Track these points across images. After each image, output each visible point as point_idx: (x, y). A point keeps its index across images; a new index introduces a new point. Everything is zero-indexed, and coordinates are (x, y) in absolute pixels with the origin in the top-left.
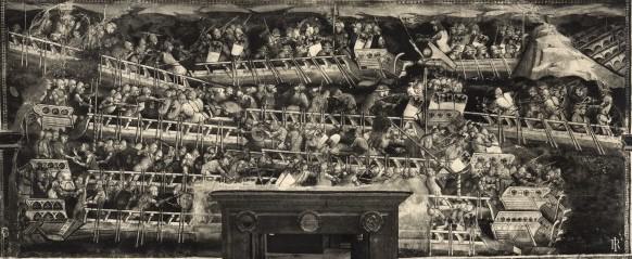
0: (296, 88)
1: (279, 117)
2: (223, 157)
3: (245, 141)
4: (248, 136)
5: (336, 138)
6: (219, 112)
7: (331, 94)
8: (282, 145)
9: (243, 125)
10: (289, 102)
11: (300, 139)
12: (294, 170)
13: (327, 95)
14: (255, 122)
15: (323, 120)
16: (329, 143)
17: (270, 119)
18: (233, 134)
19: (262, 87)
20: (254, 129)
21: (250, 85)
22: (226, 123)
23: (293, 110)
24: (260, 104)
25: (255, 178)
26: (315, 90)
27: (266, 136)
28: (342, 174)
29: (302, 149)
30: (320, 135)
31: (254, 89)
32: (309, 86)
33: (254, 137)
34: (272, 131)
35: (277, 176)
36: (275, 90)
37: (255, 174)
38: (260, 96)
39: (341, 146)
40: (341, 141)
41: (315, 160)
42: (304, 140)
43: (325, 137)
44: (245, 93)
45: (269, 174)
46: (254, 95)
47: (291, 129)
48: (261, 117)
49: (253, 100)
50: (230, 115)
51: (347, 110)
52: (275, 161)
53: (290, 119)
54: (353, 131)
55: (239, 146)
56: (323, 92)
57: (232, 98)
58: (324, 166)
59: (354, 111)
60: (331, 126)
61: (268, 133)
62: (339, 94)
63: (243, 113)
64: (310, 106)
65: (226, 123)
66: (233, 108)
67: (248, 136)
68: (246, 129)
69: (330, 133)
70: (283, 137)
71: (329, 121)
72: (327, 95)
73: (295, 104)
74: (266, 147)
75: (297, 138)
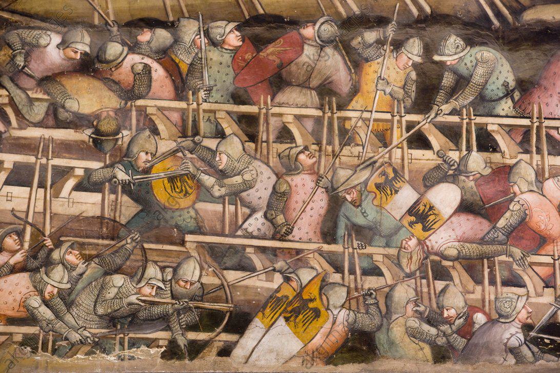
0: (308, 31)
1: (249, 126)
2: (48, 263)
3: (128, 208)
4: (140, 193)
5: (445, 197)
6: (39, 111)
7: (429, 50)
8: (256, 223)
9: (125, 157)
10: (278, 81)
11: (320, 202)
12: (299, 310)
13: (414, 50)
14: (165, 146)
15: (398, 136)
16: (421, 215)
17: (220, 134)
18: (86, 185)
19: (190, 30)
20: (160, 172)
21: (152, 23)
22: (66, 148)
23: (293, 107)
24: (181, 84)
25: (162, 336)
26: (371, 36)
27: (203, 193)
28: (469, 321)
29: (329, 234)
30: (387, 188)
31: (163, 36)
32: (351, 23)
33: (161, 193)
34: (222, 175)
35: (239, 323)
36: (234, 39)
37: (164, 321)
38: (184, 59)
39: (469, 225)
40: (466, 207)
41: (375, 271)
42: (335, 202)
43: (406, 196)
44: (134, 48)
45: (211, 320)
46: (164, 55)
47: (290, 167)
48: (188, 129)
49: (158, 72)
50: (77, 122)
51: (484, 103)
52: (232, 276)
53: (285, 135)
54: (504, 172)
55: (111, 229)
56: (398, 45)
57: (88, 66)
58: (403, 293)
59: (506, 106)
60: (424, 159)
61: (208, 180)
62: (453, 51)
63: (122, 113)
64: (355, 90)
65: (66, 148)
66: (88, 97)
67: (140, 193)
68: (131, 167)
69: (430, 179)
70: (260, 193)
71: (420, 141)
72: (414, 50)
73: (304, 85)
74: (199, 230)
75: (309, 207)
